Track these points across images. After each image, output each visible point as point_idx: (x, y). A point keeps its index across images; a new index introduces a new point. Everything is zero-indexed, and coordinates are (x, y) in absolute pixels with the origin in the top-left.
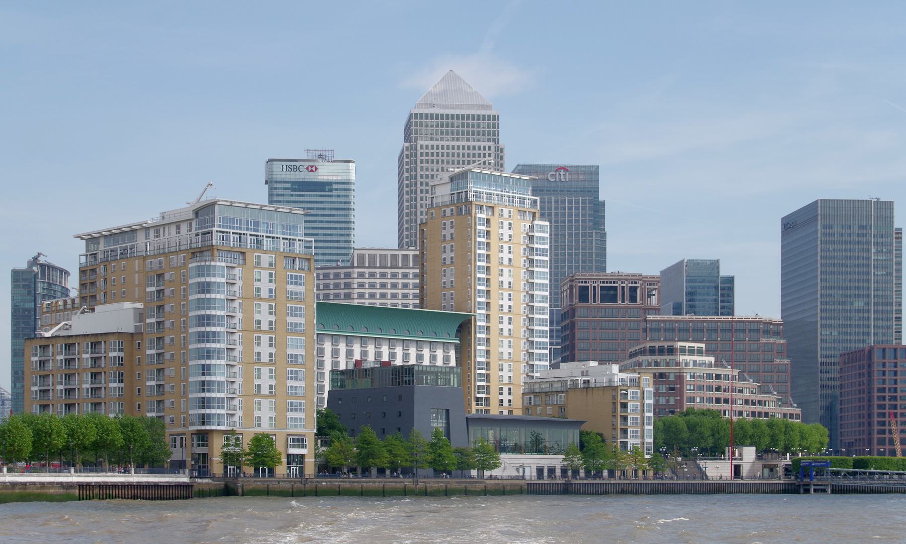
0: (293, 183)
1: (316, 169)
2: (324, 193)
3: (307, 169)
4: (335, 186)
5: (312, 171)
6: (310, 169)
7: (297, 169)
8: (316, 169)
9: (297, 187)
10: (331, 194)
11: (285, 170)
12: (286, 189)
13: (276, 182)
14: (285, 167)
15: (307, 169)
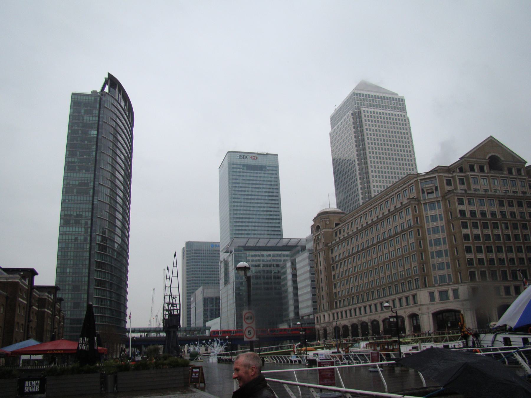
0: (244, 165)
1: (257, 158)
2: (262, 172)
3: (251, 157)
4: (268, 168)
5: (254, 159)
6: (253, 158)
7: (245, 157)
8: (257, 158)
9: (245, 168)
10: (266, 172)
11: (238, 158)
12: (239, 168)
13: (233, 164)
14: (238, 156)
15: (251, 157)
